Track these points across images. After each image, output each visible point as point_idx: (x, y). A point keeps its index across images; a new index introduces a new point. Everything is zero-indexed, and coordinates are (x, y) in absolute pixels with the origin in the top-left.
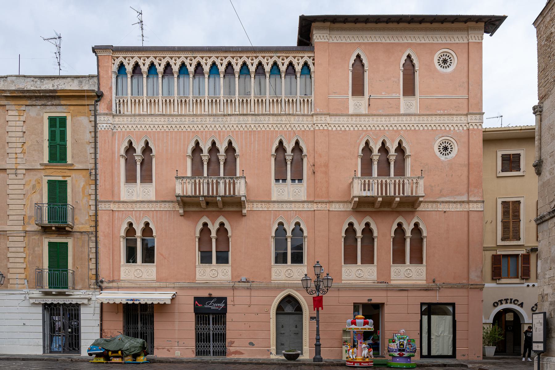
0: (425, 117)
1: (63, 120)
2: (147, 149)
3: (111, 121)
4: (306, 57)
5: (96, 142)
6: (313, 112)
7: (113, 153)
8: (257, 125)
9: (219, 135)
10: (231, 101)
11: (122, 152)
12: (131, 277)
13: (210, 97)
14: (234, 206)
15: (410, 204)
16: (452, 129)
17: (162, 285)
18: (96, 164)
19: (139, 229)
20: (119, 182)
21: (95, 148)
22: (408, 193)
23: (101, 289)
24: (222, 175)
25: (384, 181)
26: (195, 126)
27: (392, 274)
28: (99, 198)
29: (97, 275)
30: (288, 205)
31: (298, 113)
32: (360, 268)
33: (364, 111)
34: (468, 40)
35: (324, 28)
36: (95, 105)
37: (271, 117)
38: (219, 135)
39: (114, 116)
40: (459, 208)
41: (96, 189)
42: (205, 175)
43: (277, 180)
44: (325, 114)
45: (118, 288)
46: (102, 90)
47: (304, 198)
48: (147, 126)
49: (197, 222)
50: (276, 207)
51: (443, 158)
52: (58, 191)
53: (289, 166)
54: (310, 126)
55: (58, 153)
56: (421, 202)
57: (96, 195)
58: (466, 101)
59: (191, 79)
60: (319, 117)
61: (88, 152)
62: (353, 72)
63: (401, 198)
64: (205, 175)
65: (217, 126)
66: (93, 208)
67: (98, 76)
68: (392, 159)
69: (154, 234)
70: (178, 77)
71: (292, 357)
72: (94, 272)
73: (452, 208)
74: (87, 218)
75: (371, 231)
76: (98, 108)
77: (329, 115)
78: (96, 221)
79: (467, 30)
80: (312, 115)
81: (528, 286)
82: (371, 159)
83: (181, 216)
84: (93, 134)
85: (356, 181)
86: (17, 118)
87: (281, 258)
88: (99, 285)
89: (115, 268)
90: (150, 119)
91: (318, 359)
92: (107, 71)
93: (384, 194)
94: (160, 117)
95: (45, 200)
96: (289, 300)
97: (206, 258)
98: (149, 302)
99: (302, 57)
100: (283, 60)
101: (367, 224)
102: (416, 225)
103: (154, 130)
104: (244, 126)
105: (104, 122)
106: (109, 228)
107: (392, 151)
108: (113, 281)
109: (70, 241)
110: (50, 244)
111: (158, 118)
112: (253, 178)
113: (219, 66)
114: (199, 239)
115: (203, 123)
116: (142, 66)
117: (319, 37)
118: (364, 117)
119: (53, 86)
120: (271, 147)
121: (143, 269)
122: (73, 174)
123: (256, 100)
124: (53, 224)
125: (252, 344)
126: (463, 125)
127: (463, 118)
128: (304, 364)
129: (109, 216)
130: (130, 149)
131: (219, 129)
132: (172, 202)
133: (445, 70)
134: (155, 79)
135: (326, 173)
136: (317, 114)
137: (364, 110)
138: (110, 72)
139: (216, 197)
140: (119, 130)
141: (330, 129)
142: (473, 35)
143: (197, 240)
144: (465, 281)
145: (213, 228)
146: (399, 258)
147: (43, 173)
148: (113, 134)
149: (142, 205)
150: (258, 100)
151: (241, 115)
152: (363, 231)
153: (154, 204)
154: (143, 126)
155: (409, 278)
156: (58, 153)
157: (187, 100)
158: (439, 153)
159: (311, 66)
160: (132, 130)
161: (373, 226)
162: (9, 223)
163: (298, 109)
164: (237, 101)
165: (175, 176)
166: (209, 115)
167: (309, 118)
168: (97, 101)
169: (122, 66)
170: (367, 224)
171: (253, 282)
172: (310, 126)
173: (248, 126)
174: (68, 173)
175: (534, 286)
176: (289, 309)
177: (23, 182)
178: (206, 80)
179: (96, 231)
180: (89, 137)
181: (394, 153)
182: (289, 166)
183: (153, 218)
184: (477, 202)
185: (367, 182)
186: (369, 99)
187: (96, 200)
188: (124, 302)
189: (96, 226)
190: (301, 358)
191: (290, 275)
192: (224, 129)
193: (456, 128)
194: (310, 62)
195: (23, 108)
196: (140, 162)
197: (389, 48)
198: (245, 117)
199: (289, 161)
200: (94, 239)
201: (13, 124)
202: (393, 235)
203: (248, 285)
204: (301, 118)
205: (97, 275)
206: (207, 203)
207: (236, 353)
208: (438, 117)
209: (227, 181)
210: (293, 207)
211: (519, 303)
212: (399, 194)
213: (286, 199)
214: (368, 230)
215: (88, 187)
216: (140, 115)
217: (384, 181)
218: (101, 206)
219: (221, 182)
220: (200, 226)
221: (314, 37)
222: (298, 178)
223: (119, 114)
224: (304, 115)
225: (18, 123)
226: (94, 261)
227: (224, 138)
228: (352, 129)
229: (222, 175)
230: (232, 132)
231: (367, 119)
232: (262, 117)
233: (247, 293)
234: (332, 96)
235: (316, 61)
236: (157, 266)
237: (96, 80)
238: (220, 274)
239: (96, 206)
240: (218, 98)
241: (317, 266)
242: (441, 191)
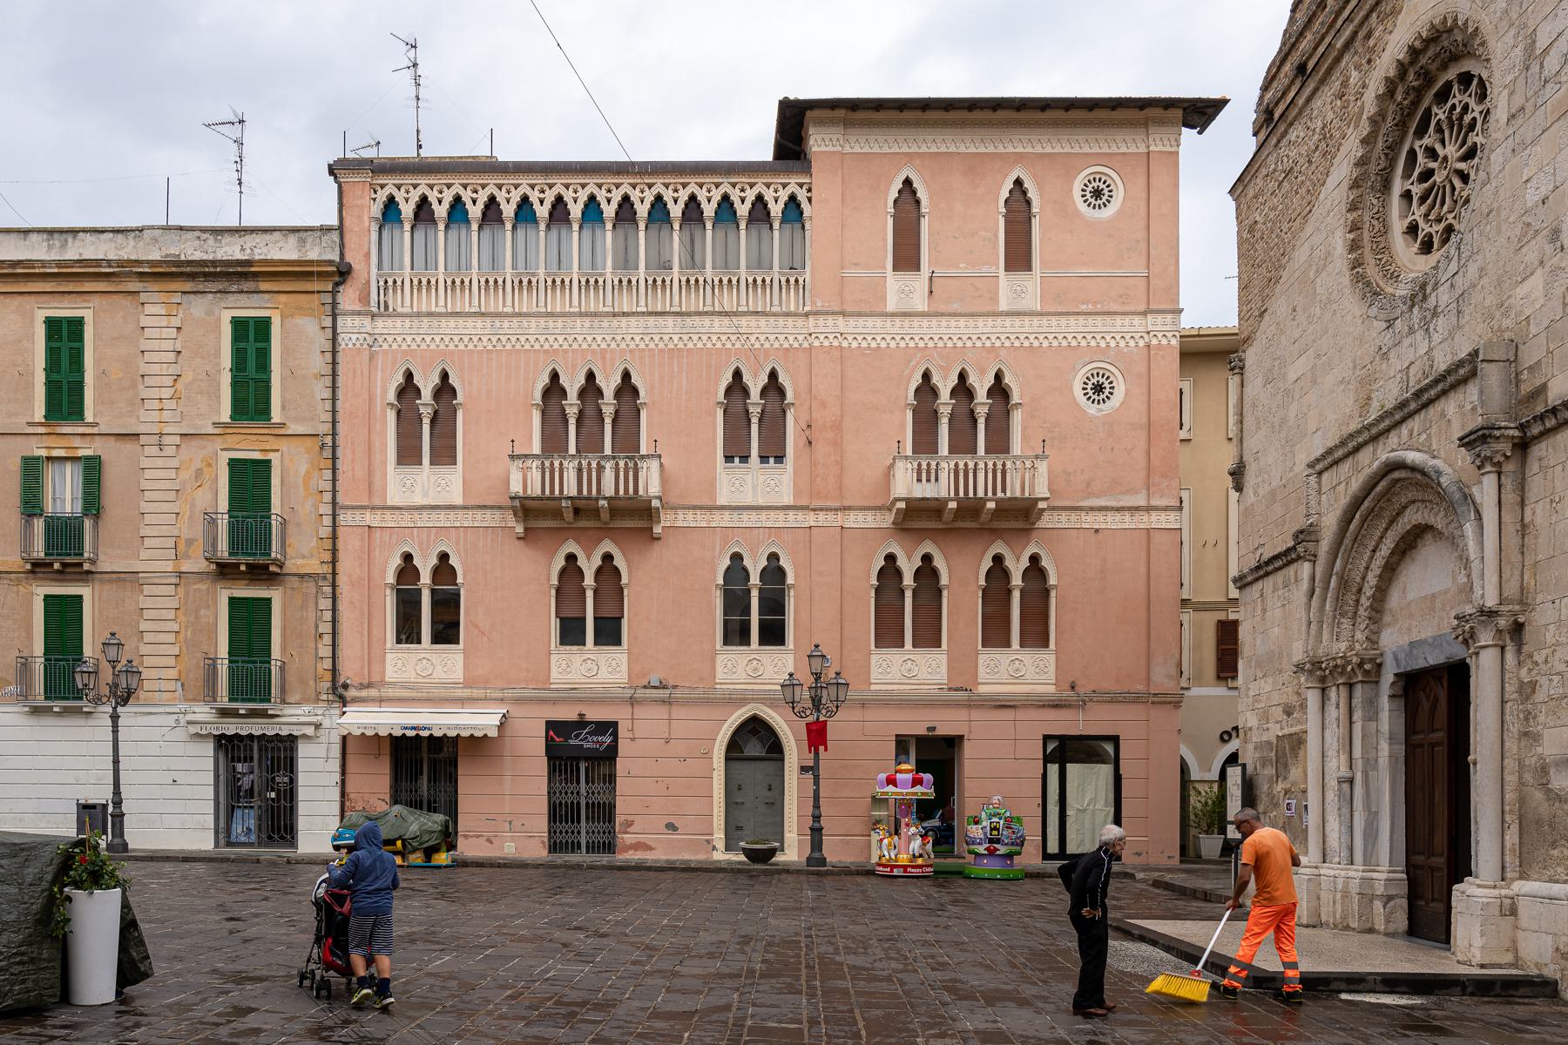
0: (1053, 318)
1: (263, 326)
2: (445, 389)
3: (369, 329)
5: (334, 375)
6: (807, 309)
7: (371, 399)
8: (685, 337)
9: (604, 359)
10: (630, 281)
11: (391, 396)
12: (409, 675)
13: (583, 275)
14: (635, 518)
15: (1020, 516)
16: (1113, 344)
18: (334, 422)
19: (425, 566)
20: (384, 463)
21: (334, 388)
22: (1014, 490)
23: (344, 701)
24: (608, 451)
25: (961, 465)
26: (551, 339)
27: (981, 669)
28: (340, 499)
29: (334, 670)
30: (754, 515)
31: (776, 309)
33: (921, 304)
35: (832, 122)
36: (334, 293)
37: (716, 319)
38: (604, 359)
39: (373, 316)
40: (1127, 521)
41: (334, 480)
42: (572, 450)
43: (729, 458)
44: (833, 313)
45: (381, 701)
46: (348, 259)
47: (788, 500)
48: (447, 339)
49: (554, 553)
50: (725, 519)
51: (1092, 409)
52: (250, 482)
53: (755, 428)
54: (800, 338)
55: (251, 399)
56: (1043, 510)
57: (334, 491)
58: (1142, 283)
59: (542, 234)
60: (821, 318)
61: (319, 398)
62: (894, 217)
63: (998, 501)
64: (572, 450)
65: (599, 338)
66: (327, 521)
67: (341, 228)
68: (982, 412)
69: (460, 580)
70: (514, 227)
71: (761, 856)
72: (328, 664)
73: (1112, 521)
74: (314, 543)
75: (935, 573)
76: (340, 298)
77: (843, 314)
78: (334, 551)
79: (1145, 124)
80: (807, 315)
84: (328, 357)
85: (900, 464)
87: (736, 634)
88: (340, 695)
89: (374, 657)
90: (452, 322)
91: (816, 859)
92: (360, 217)
93: (961, 494)
95: (223, 504)
96: (755, 728)
97: (571, 632)
98: (452, 734)
99: (784, 186)
100: (743, 190)
101: (927, 558)
102: (1035, 559)
103: (461, 347)
104: (656, 338)
105: (353, 330)
107: (981, 395)
108: (369, 686)
109: (276, 595)
110: (232, 600)
111: (470, 320)
112: (678, 453)
113: (604, 205)
114: (558, 590)
116: (435, 206)
117: (820, 142)
119: (243, 249)
120: (717, 383)
121: (434, 658)
122: (284, 445)
123: (684, 280)
124: (243, 559)
125: (671, 827)
126: (1137, 336)
127: (1137, 320)
128: (787, 870)
130: (408, 388)
131: (604, 346)
132: (500, 508)
133: (1097, 214)
134: (463, 232)
135: (837, 444)
136: (816, 313)
138: (366, 219)
139: (597, 499)
140: (385, 346)
141: (845, 344)
142: (1158, 137)
143: (553, 592)
144: (1140, 687)
145: (589, 566)
146: (995, 633)
147: (218, 443)
149: (434, 514)
150: (688, 281)
151: (650, 314)
152: (918, 574)
153: (461, 512)
154: (437, 339)
155: (1017, 679)
156: (251, 399)
157: (534, 280)
159: (805, 205)
160: (414, 347)
161: (939, 563)
162: (144, 554)
163: (776, 301)
164: (642, 282)
165: (503, 449)
166: (581, 314)
167: (800, 322)
168: (337, 284)
169: (391, 202)
170: (927, 558)
171: (675, 687)
172: (800, 338)
173: (666, 338)
174: (273, 443)
176: (754, 748)
177: (175, 463)
178: (575, 235)
179: (334, 574)
180: (320, 363)
182: (755, 428)
183: (458, 543)
184: (1166, 509)
185: (924, 466)
186: (931, 278)
187: (334, 503)
188: (398, 733)
189: (334, 562)
190: (779, 858)
191: (756, 672)
192: (613, 345)
193: (1122, 344)
194: (802, 196)
195: (177, 298)
196: (428, 418)
197: (974, 165)
198: (660, 319)
199: (755, 416)
200: (329, 590)
201: (154, 333)
202: (982, 582)
203: (665, 694)
204: (781, 320)
205: (334, 670)
206: (577, 511)
207: (638, 846)
208: (1081, 318)
209: (622, 463)
210: (766, 519)
212: (994, 493)
213: (749, 501)
214: (927, 571)
215: (316, 473)
216: (430, 314)
217: (961, 465)
218: (345, 518)
219: (609, 465)
220: (560, 562)
221: (811, 142)
222: (774, 453)
223: (385, 311)
224: (787, 314)
225: (167, 333)
226: (327, 639)
228: (893, 344)
229: (608, 451)
230: (631, 351)
231: (925, 322)
232: (697, 319)
233: (661, 712)
234: (850, 272)
235: (814, 194)
236: (465, 652)
237: (335, 236)
238: (603, 669)
239: (334, 516)
240: (601, 275)
241: (816, 655)
242: (1088, 484)
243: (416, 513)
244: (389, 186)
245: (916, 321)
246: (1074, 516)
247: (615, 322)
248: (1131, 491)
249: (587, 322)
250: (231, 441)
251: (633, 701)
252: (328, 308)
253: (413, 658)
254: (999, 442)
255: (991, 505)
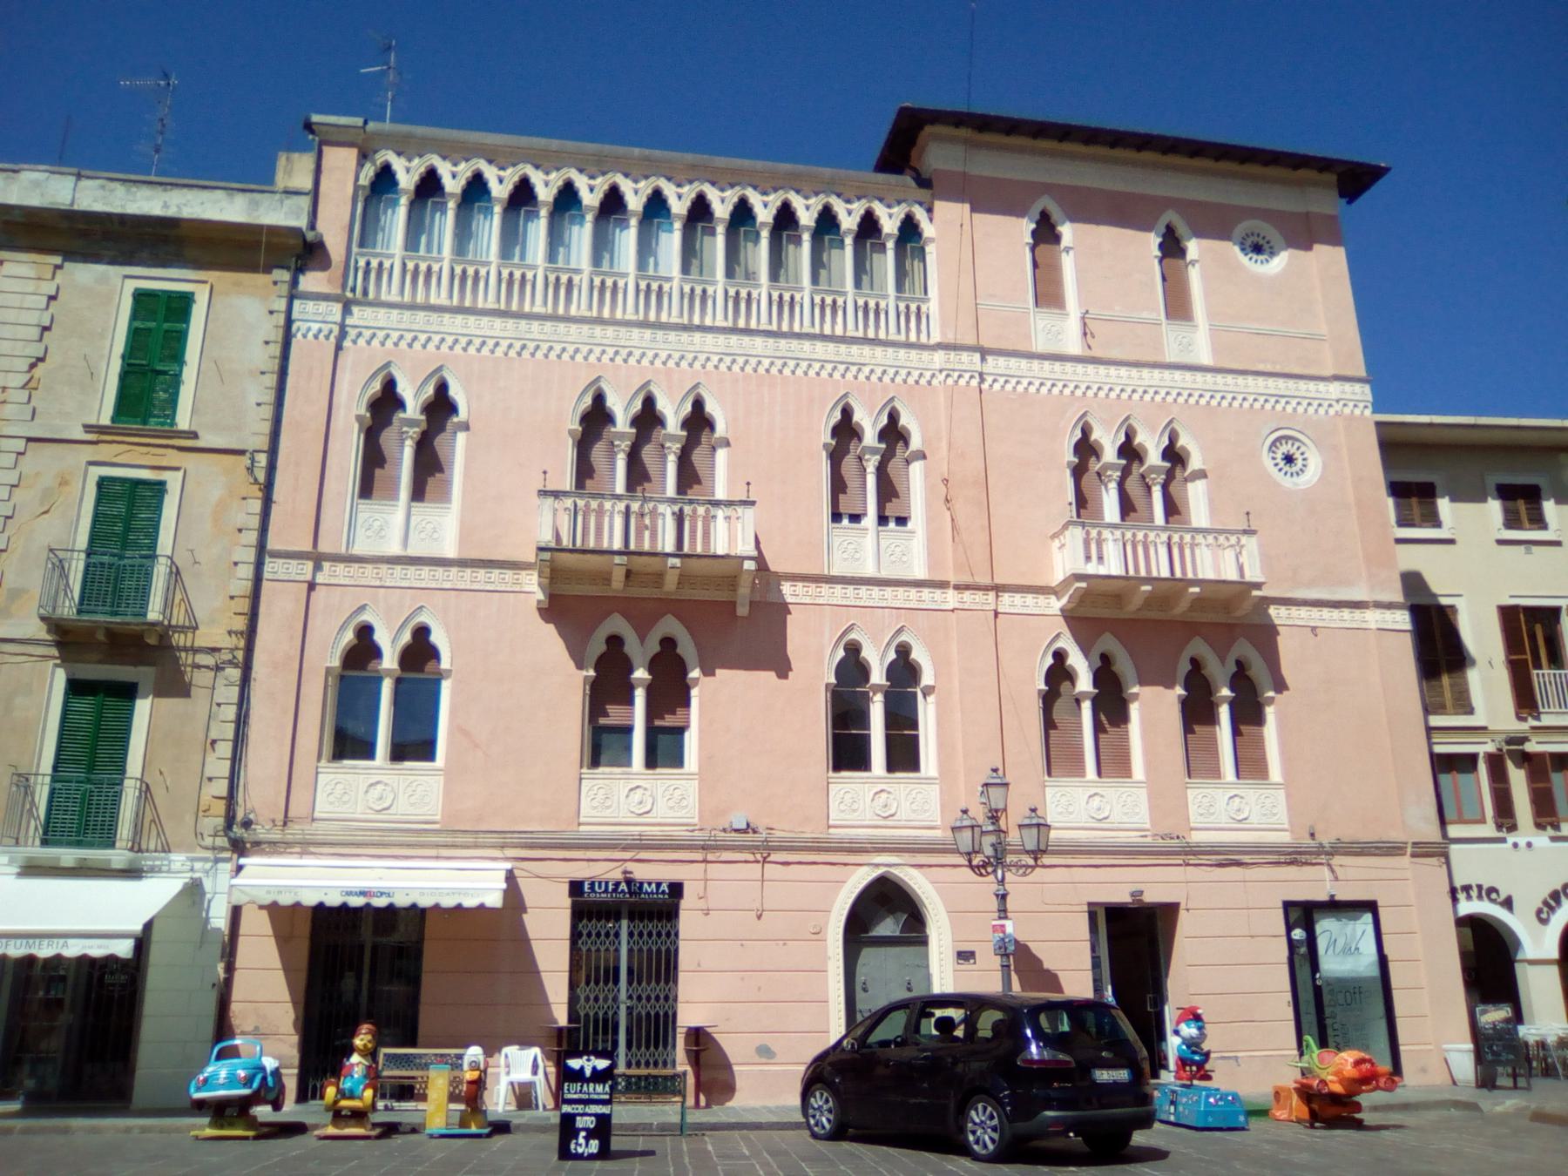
1: (180, 305)
27: (1192, 809)
29: (231, 798)
30: (876, 591)
32: (1098, 790)
33: (1074, 347)
45: (306, 846)
51: (1287, 482)
52: (127, 513)
66: (247, 571)
72: (221, 788)
79: (1300, 184)
81: (1515, 845)
84: (276, 350)
86: (31, 286)
105: (316, 318)
111: (485, 319)
119: (166, 206)
122: (188, 460)
147: (89, 453)
158: (1276, 469)
170: (1105, 658)
174: (172, 458)
175: (1529, 845)
186: (1083, 318)
204: (902, 352)
205: (231, 798)
210: (890, 595)
211: (1503, 896)
213: (869, 571)
218: (271, 567)
226: (225, 749)
231: (1080, 368)
238: (661, 803)
243: (384, 567)
245: (1069, 366)
247: (685, 336)
249: (648, 333)
250: (105, 452)
252: (284, 289)
253: (362, 781)
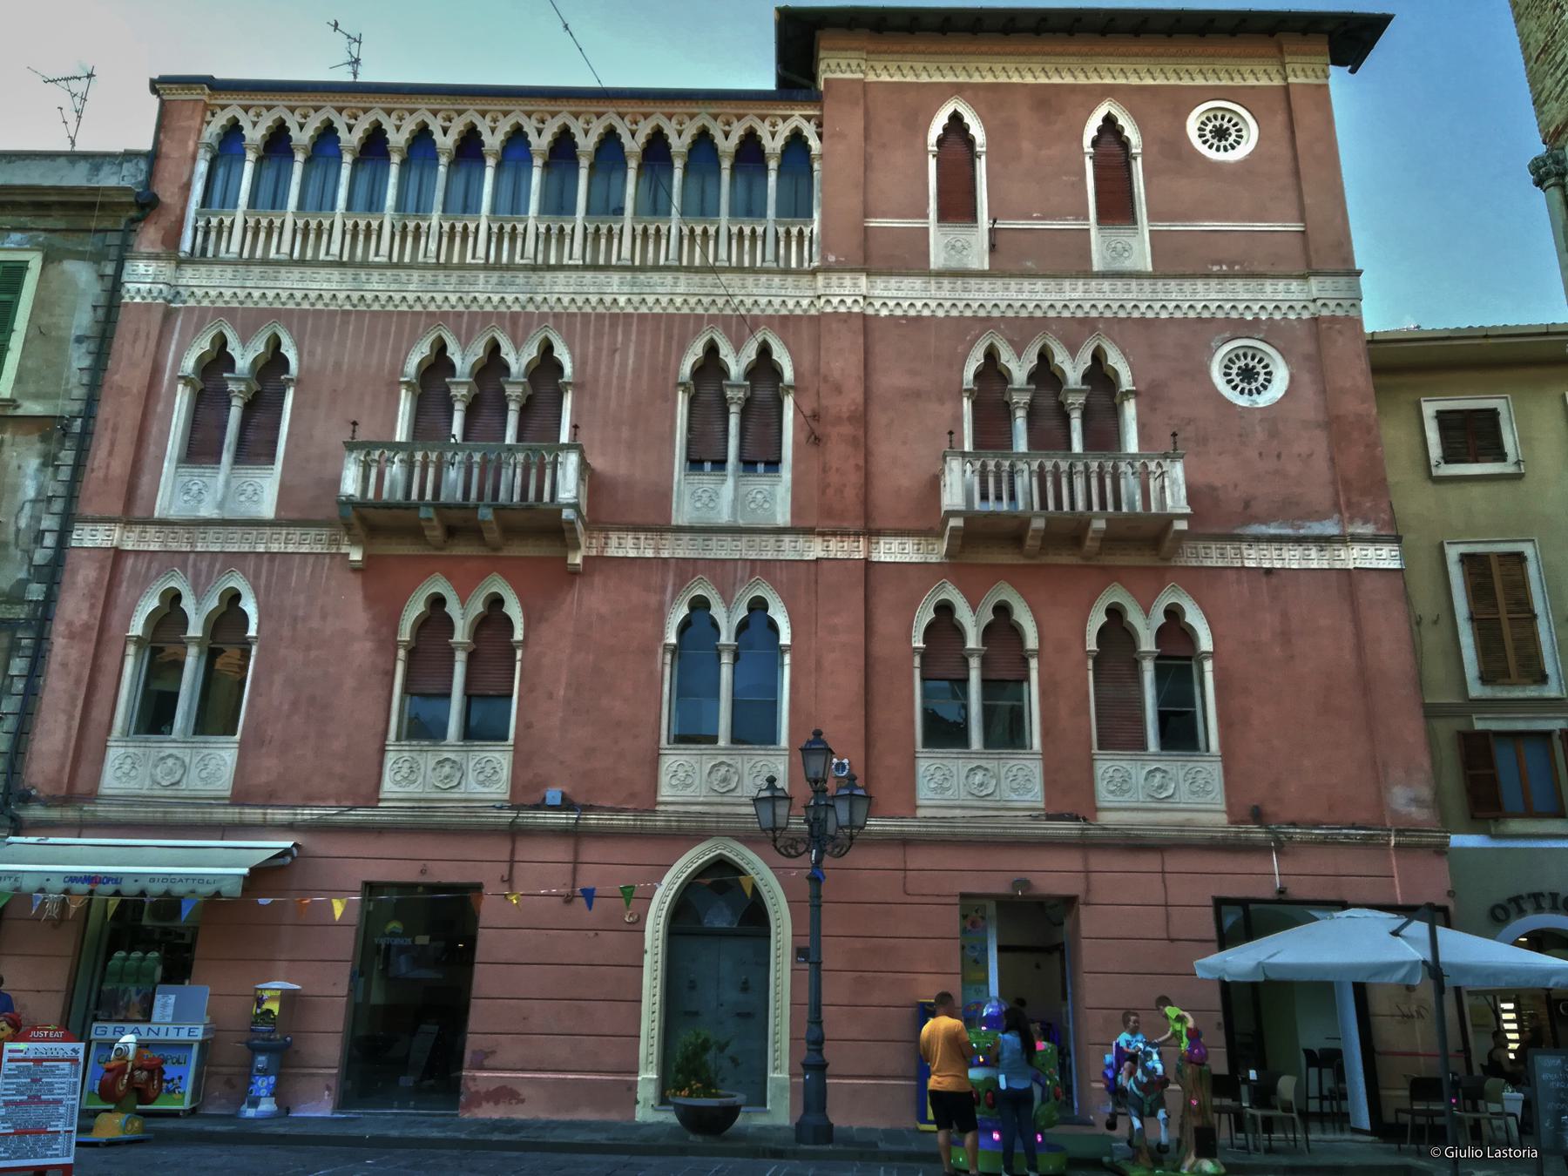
4: (798, 118)
6: (815, 264)
12: (138, 784)
15: (1146, 543)
17: (253, 814)
32: (983, 763)
34: (1286, 79)
37: (682, 276)
40: (1315, 559)
43: (694, 463)
44: (852, 271)
53: (734, 421)
73: (1292, 558)
80: (814, 272)
82: (1007, 404)
83: (355, 570)
85: (955, 465)
90: (296, 272)
94: (328, 270)
100: (728, 124)
101: (1003, 610)
106: (92, 606)
115: (466, 288)
118: (979, 281)
127: (1295, 285)
129: (102, 568)
137: (979, 258)
139: (476, 507)
142: (1298, 67)
146: (1120, 732)
148: (169, 315)
152: (988, 633)
158: (1229, 387)
159: (814, 143)
161: (1024, 618)
166: (486, 267)
167: (805, 281)
168: (134, 221)
176: (720, 918)
181: (1079, 386)
182: (734, 421)
183: (257, 576)
186: (992, 231)
194: (809, 131)
199: (734, 411)
204: (777, 280)
206: (451, 532)
207: (504, 1094)
208: (1213, 283)
214: (1002, 627)
221: (822, 66)
223: (198, 258)
227: (526, 333)
231: (986, 284)
234: (874, 223)
235: (825, 130)
240: (521, 221)
242: (1247, 505)
244: (233, 108)
245: (973, 283)
246: (1229, 549)
247: (535, 277)
248: (1321, 517)
251: (514, 832)
253: (154, 754)
254: (1103, 436)
255: (1100, 524)
